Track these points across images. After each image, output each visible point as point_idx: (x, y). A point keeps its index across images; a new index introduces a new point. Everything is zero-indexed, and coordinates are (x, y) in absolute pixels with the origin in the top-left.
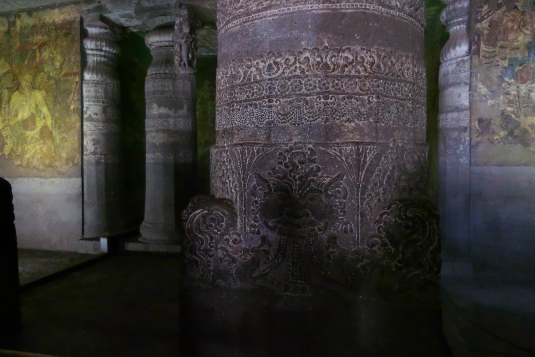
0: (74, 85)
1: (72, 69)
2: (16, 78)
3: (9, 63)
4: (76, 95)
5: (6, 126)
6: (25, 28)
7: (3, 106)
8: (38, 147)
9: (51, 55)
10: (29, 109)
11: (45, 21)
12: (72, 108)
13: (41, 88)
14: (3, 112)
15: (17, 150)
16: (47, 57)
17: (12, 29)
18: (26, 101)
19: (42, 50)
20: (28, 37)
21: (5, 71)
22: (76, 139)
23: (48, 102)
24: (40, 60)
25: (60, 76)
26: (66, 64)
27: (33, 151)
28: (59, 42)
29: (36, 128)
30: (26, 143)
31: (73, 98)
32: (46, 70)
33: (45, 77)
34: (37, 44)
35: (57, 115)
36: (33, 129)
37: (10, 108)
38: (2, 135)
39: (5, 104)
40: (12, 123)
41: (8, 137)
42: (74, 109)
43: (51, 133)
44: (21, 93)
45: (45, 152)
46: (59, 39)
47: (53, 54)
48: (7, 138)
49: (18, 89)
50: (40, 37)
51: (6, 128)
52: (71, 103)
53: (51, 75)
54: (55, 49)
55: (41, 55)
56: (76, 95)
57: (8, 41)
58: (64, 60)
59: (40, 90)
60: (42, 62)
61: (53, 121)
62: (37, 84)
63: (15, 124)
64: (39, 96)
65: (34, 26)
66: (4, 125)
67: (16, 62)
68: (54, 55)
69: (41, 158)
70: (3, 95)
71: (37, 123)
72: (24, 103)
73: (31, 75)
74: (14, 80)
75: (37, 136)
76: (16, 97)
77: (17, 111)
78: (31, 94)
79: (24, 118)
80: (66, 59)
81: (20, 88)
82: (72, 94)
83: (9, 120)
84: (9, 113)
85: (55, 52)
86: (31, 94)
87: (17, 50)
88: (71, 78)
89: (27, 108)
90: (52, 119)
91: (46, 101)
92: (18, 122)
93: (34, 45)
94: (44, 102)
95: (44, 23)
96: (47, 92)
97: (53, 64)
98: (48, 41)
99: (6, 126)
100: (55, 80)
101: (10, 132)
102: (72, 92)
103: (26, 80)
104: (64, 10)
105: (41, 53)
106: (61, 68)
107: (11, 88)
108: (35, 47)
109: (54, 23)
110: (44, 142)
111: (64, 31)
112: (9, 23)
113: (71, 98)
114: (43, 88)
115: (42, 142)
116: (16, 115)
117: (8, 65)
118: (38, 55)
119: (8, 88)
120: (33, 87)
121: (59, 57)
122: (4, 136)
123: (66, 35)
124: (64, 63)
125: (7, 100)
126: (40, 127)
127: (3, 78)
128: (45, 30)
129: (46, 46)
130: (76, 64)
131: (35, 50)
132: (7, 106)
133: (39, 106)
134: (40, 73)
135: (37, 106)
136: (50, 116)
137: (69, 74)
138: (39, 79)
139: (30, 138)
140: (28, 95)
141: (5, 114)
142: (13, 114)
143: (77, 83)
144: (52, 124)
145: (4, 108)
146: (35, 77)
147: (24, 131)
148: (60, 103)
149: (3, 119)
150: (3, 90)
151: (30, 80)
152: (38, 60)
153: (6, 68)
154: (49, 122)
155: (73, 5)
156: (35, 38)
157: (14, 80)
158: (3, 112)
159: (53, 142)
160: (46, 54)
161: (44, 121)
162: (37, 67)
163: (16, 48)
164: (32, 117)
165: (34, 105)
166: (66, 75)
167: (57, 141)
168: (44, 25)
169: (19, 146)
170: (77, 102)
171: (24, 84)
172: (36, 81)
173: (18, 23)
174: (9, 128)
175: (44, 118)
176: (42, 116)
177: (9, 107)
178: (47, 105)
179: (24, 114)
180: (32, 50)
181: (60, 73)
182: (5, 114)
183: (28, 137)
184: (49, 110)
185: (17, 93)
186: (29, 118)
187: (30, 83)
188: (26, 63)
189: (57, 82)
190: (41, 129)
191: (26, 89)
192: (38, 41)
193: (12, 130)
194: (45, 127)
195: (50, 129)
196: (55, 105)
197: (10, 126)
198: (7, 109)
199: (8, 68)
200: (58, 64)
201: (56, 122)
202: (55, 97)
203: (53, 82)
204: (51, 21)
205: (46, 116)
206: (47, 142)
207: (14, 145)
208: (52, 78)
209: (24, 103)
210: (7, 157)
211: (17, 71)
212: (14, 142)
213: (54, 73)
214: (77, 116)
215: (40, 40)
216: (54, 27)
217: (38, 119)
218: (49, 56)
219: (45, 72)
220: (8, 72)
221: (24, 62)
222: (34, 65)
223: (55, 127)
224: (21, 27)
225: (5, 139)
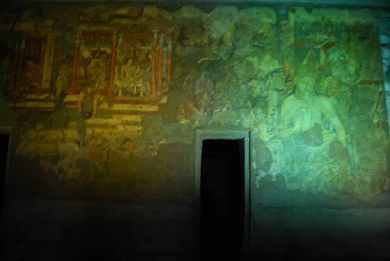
0: (376, 96)
1: (373, 77)
2: (290, 79)
3: (279, 60)
4: (380, 107)
5: (274, 138)
6: (303, 24)
7: (270, 112)
8: (326, 167)
9: (342, 58)
10: (311, 118)
11: (331, 20)
12: (375, 121)
13: (329, 94)
14: (270, 120)
15: (292, 170)
16: (336, 59)
17: (283, 22)
18: (307, 109)
19: (329, 50)
20: (307, 33)
21: (272, 68)
22: (385, 159)
23: (340, 112)
24: (326, 62)
25: (357, 83)
26: (363, 70)
27: (318, 173)
28: (352, 44)
29: (322, 143)
30: (306, 161)
31: (376, 110)
32: (335, 73)
33: (335, 83)
34: (321, 43)
35: (353, 128)
36: (319, 145)
37: (282, 114)
38: (267, 150)
39: (273, 110)
40: (285, 134)
41: (278, 153)
42: (378, 123)
43: (346, 150)
44: (299, 98)
45: (336, 174)
46: (351, 42)
47: (345, 57)
48: (275, 152)
49: (293, 92)
50: (325, 37)
51: (276, 140)
52: (374, 115)
53: (343, 80)
54: (347, 52)
55: (327, 57)
56: (380, 107)
57: (277, 35)
58: (361, 66)
59: (327, 96)
60: (328, 64)
61: (348, 136)
62: (323, 90)
63: (290, 136)
64: (326, 104)
65: (316, 24)
66: (272, 136)
67: (289, 60)
68: (347, 59)
69: (331, 182)
70: (268, 98)
71: (324, 136)
72: (304, 110)
73: (312, 77)
74: (287, 81)
75: (325, 153)
76: (290, 103)
77: (292, 119)
78: (313, 101)
79: (304, 130)
80: (364, 64)
81: (297, 92)
82: (375, 106)
83: (279, 130)
84: (279, 121)
85: (347, 55)
86: (313, 101)
87: (291, 46)
88: (372, 87)
89: (307, 117)
90: (346, 133)
91: (337, 110)
92: (294, 134)
93: (318, 45)
94: (334, 111)
95: (329, 22)
96: (339, 100)
97: (345, 69)
98: (337, 42)
99: (274, 138)
100: (349, 86)
101: (282, 146)
102: (374, 103)
103: (305, 83)
104: (355, 12)
105: (327, 56)
106: (357, 73)
107: (282, 90)
108: (319, 47)
109: (343, 24)
110: (336, 161)
111: (358, 34)
112: (278, 16)
113: (373, 110)
114: (332, 95)
115: (331, 160)
116: (292, 125)
117: (276, 62)
118: (323, 56)
119: (278, 90)
120: (317, 93)
121: (353, 62)
122: (271, 150)
123: (362, 39)
124: (360, 70)
125: (276, 104)
126: (329, 142)
127: (270, 77)
128: (332, 29)
129: (334, 47)
130: (378, 72)
131: (318, 50)
132: (276, 112)
133: (327, 116)
134: (327, 76)
135: (323, 115)
136: (342, 129)
137: (370, 83)
138: (325, 83)
139: (313, 156)
140: (310, 101)
141: (273, 122)
142: (286, 122)
143: (381, 93)
144: (347, 139)
145: (272, 115)
146: (318, 81)
147: (304, 146)
148: (358, 115)
149: (270, 129)
150: (270, 92)
151: (313, 84)
152: (322, 61)
153: (273, 65)
154: (342, 137)
155: (368, 10)
156: (318, 36)
157: (287, 81)
158: (270, 120)
159: (349, 162)
160: (334, 56)
161: (334, 135)
162: (321, 69)
163: (289, 43)
164: (317, 129)
165: (318, 115)
166: (363, 83)
167: (356, 161)
168: (329, 25)
169: (296, 165)
170: (382, 115)
171: (302, 87)
172: (320, 85)
173: (292, 17)
174: (280, 141)
175: (335, 131)
176: (332, 128)
177: (280, 113)
178: (339, 115)
179: (304, 123)
180: (314, 49)
181: (356, 80)
182: (273, 122)
183: (309, 153)
184: (342, 122)
185: (292, 97)
186: (311, 129)
187: (312, 88)
188: (305, 63)
189: (353, 89)
190: (331, 145)
191: (307, 93)
192: (322, 40)
193: (283, 143)
194: (337, 142)
195: (344, 145)
196: (350, 117)
197: (281, 138)
198: (276, 116)
199: (276, 65)
200: (352, 69)
201: (352, 137)
202: (351, 107)
203: (347, 89)
204: (339, 21)
205: (337, 129)
206: (339, 161)
207: (287, 164)
208: (345, 84)
209: (304, 110)
210: (274, 179)
211: (292, 71)
212: (287, 160)
213: (348, 78)
214: (383, 131)
215: (326, 40)
216: (343, 28)
217: (325, 131)
218: (339, 59)
219: (333, 76)
220: (277, 71)
221: (302, 61)
222: (317, 66)
223: (351, 143)
224: (296, 22)
225: (273, 155)
